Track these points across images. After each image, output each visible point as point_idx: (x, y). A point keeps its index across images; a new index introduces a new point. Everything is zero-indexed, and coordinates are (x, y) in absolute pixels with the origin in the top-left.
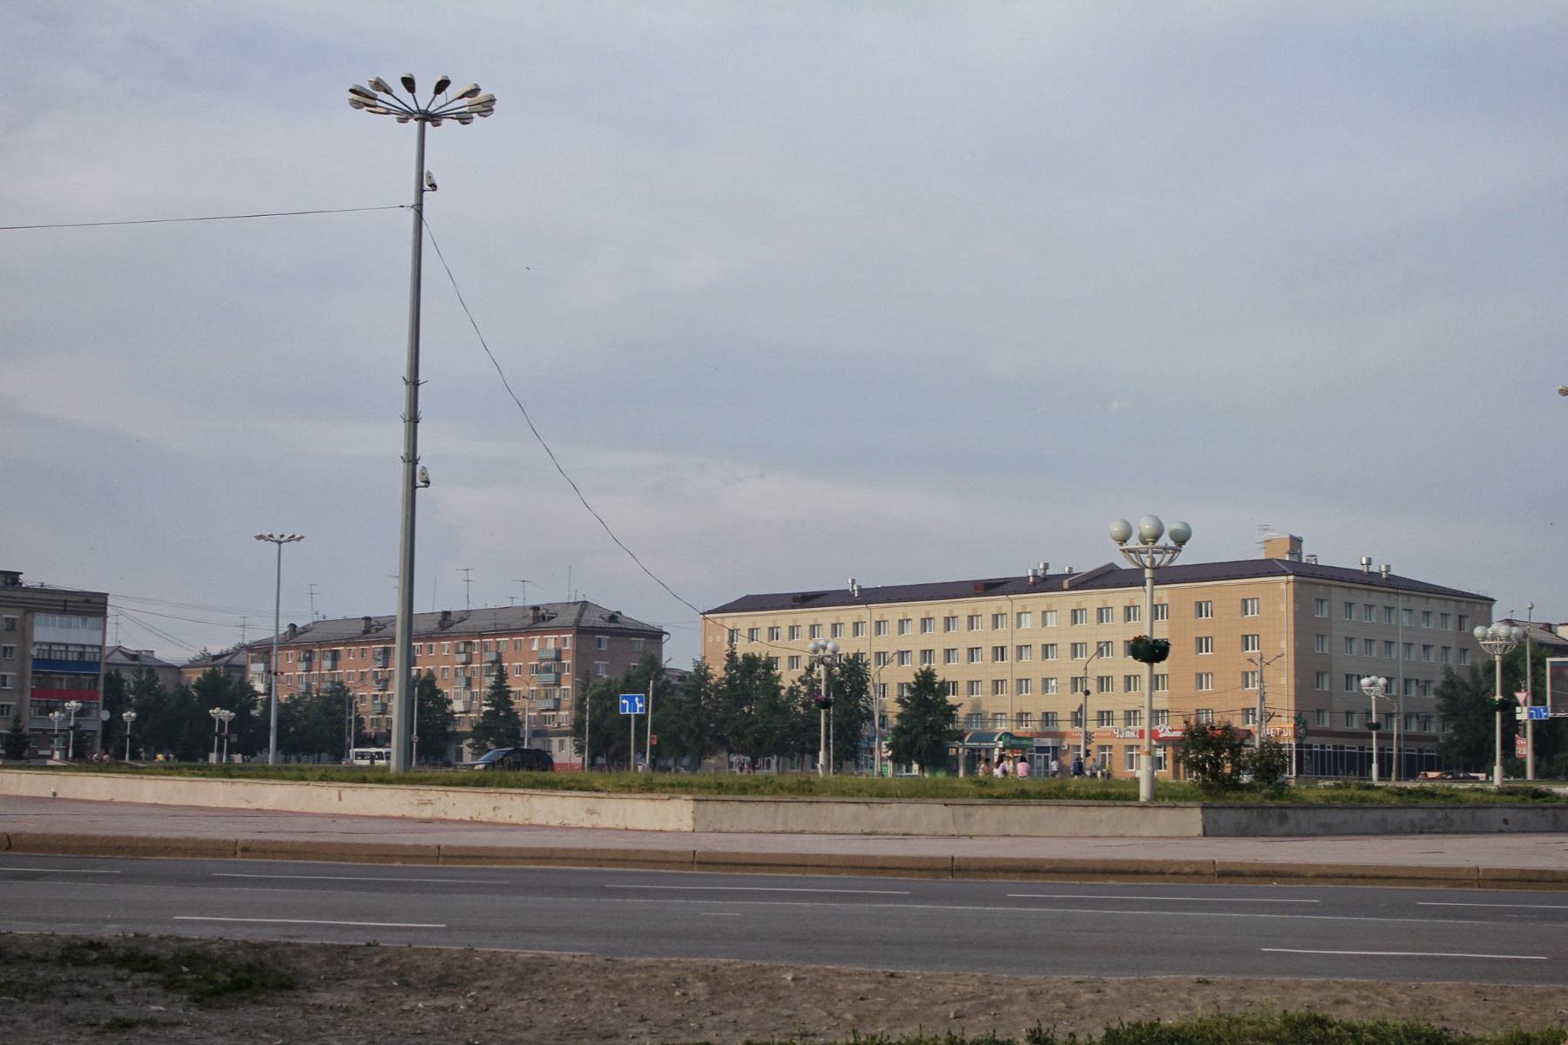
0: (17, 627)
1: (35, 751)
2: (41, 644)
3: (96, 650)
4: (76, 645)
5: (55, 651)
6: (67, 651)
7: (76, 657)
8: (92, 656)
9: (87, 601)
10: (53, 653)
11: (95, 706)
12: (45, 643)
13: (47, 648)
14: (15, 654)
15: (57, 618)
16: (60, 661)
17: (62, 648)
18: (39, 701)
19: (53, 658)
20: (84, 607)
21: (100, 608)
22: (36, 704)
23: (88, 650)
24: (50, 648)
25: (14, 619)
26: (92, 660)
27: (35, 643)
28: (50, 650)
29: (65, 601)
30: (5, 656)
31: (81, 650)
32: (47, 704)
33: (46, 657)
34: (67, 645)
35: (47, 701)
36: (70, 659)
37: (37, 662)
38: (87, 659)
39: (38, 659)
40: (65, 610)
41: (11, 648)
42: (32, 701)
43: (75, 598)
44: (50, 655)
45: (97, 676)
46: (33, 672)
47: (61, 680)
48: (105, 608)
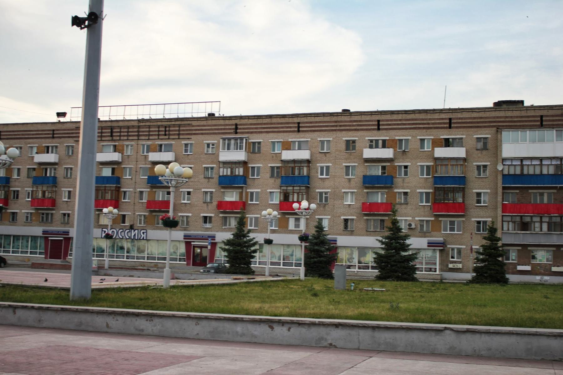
0: (489, 146)
1: (515, 265)
2: (512, 159)
5: (528, 165)
6: (541, 165)
7: (552, 171)
10: (525, 168)
13: (519, 163)
14: (488, 172)
16: (534, 175)
18: (512, 216)
19: (525, 172)
22: (509, 219)
27: (504, 160)
28: (522, 166)
30: (479, 174)
31: (554, 162)
33: (518, 172)
34: (541, 159)
36: (545, 172)
37: (506, 177)
39: (509, 175)
41: (485, 166)
42: (503, 216)
43: (551, 112)
44: (522, 170)
46: (504, 188)
47: (542, 195)
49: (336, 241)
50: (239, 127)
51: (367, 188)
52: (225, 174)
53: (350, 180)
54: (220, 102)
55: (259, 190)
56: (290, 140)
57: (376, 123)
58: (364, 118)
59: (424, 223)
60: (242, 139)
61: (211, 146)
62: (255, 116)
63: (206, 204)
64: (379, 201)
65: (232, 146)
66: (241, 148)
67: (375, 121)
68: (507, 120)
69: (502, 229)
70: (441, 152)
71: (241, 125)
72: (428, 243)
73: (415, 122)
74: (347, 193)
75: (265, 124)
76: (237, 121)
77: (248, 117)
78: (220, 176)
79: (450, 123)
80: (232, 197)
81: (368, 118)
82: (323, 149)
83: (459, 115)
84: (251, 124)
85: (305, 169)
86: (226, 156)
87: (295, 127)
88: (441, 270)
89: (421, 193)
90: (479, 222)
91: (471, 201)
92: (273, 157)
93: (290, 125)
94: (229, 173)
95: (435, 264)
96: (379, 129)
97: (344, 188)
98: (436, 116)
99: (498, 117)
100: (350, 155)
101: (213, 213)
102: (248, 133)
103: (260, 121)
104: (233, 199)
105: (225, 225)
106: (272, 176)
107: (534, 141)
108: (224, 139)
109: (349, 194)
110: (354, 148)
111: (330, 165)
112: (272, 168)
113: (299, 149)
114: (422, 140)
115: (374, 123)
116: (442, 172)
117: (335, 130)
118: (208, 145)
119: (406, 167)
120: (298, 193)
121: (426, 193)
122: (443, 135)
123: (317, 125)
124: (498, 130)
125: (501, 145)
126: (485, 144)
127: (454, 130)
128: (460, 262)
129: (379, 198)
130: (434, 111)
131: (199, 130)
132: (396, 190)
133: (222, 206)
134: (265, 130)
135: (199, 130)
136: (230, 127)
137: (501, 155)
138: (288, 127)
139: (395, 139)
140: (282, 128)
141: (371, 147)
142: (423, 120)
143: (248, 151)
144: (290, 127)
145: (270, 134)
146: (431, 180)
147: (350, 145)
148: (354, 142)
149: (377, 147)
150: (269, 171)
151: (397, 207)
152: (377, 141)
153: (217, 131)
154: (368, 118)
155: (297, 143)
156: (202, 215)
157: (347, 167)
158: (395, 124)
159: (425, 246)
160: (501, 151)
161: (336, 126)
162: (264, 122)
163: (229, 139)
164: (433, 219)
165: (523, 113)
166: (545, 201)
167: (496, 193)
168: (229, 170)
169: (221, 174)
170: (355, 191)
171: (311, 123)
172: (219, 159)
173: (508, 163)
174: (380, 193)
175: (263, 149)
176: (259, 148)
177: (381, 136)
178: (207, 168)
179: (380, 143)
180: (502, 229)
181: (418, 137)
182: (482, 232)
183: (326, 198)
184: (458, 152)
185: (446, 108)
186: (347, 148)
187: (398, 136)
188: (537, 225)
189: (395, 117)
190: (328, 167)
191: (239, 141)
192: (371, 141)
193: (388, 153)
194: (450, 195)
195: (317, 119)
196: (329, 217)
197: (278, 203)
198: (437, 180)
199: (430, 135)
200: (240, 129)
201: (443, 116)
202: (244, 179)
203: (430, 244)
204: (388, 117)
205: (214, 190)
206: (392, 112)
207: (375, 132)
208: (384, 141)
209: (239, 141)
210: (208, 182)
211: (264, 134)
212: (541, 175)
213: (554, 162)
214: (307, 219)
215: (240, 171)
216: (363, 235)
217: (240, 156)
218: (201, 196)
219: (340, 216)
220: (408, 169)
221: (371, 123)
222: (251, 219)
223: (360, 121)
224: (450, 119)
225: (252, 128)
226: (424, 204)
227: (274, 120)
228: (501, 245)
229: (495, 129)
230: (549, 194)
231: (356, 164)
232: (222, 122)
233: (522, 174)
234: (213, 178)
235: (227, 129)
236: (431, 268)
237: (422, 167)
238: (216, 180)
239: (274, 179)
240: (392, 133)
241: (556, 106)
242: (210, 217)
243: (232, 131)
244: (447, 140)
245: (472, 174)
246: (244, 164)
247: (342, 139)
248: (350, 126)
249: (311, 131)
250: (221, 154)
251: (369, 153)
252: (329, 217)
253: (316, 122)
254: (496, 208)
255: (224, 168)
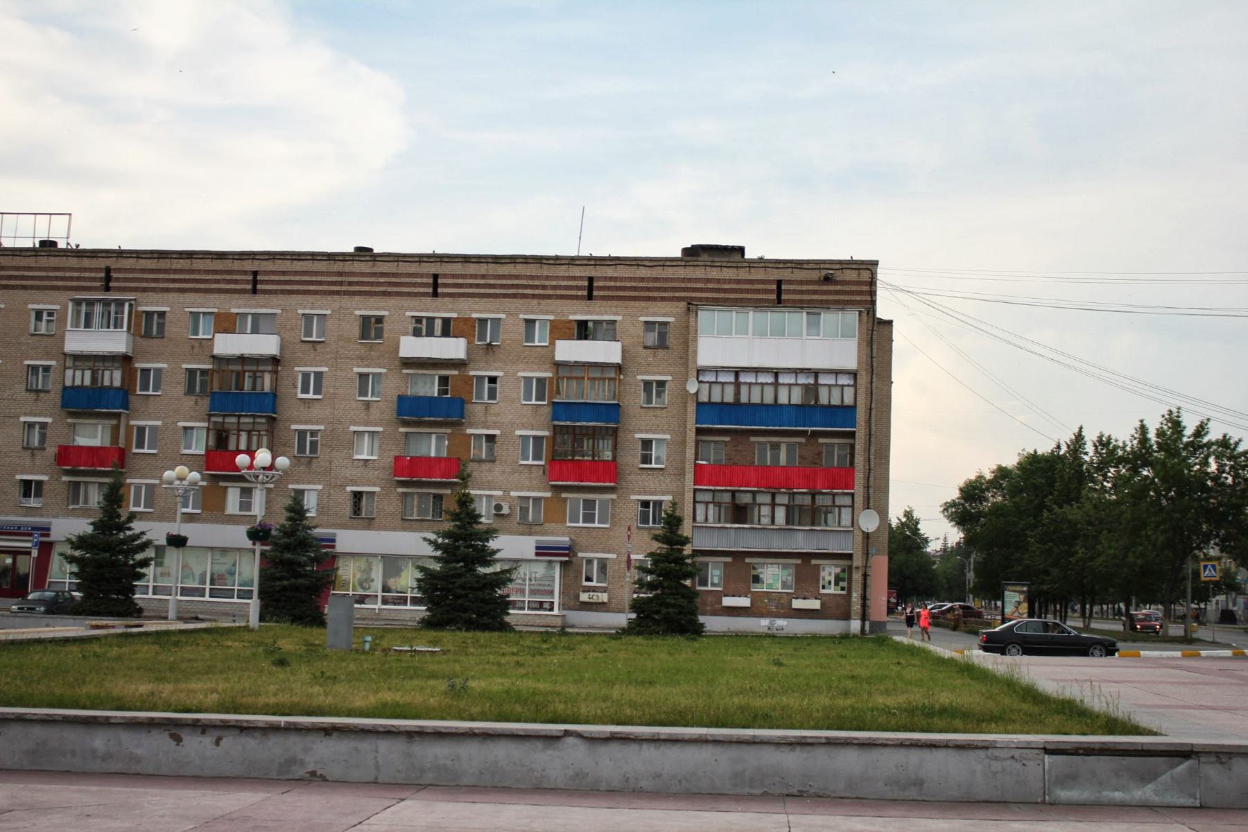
0: (671, 340)
1: (719, 596)
2: (717, 370)
3: (844, 380)
4: (796, 372)
5: (750, 384)
6: (776, 384)
7: (797, 398)
8: (836, 393)
9: (827, 280)
10: (744, 390)
11: (847, 501)
12: (725, 369)
13: (731, 379)
14: (666, 397)
15: (752, 316)
16: (762, 405)
17: (770, 379)
18: (714, 491)
19: (744, 399)
20: (815, 292)
21: (860, 293)
22: (708, 497)
23: (823, 380)
24: (737, 374)
25: (665, 324)
26: (836, 401)
27: (700, 371)
28: (737, 385)
29: (779, 283)
30: (649, 401)
31: (802, 380)
32: (733, 496)
33: (729, 398)
34: (776, 373)
35: (733, 492)
36: (783, 399)
37: (703, 407)
38: (824, 400)
39: (710, 403)
40: (779, 301)
41: (661, 384)
43: (799, 275)
44: (737, 393)
45: (852, 435)
46: (699, 432)
47: (776, 447)
48: (873, 293)
49: (334, 541)
50: (114, 275)
51: (406, 424)
52: (78, 382)
53: (368, 405)
54: (70, 214)
55: (159, 423)
56: (234, 310)
57: (431, 281)
58: (404, 268)
59: (529, 503)
60: (120, 303)
61: (45, 317)
62: (152, 252)
63: (29, 453)
64: (433, 454)
65: (96, 319)
66: (118, 324)
67: (427, 275)
68: (710, 286)
69: (694, 519)
70: (569, 350)
71: (119, 270)
72: (537, 548)
73: (515, 282)
74: (362, 433)
75: (176, 271)
76: (111, 263)
77: (138, 254)
78: (65, 388)
79: (590, 288)
80: (92, 436)
81: (412, 268)
82: (309, 334)
83: (610, 272)
84: (143, 271)
85: (267, 379)
86: (79, 341)
87: (247, 282)
88: (564, 606)
89: (525, 438)
90: (645, 504)
91: (631, 458)
92: (193, 348)
93: (235, 277)
94: (87, 382)
95: (551, 593)
96: (435, 294)
97: (355, 424)
98: (562, 271)
99: (690, 280)
100: (371, 347)
101: (46, 474)
102: (136, 290)
103: (164, 264)
104: (96, 442)
105: (76, 501)
106: (190, 390)
107: (762, 334)
108: (78, 303)
109: (366, 435)
110: (379, 334)
111: (325, 369)
112: (191, 372)
113: (255, 330)
114: (530, 323)
115: (425, 280)
116: (570, 393)
117: (338, 293)
118: (39, 315)
119: (493, 380)
120: (249, 432)
121: (535, 437)
122: (575, 313)
123: (297, 278)
124: (692, 306)
125: (696, 340)
126: (662, 336)
127: (599, 303)
128: (604, 590)
129: (432, 446)
130: (557, 260)
131: (16, 278)
132: (469, 431)
133: (67, 456)
134: (177, 285)
135: (16, 278)
136: (93, 275)
137: (695, 361)
138: (229, 282)
139: (471, 319)
140: (217, 281)
141: (417, 333)
142: (532, 278)
143: (133, 331)
144: (236, 282)
145: (186, 295)
146: (547, 411)
147: (371, 327)
148: (380, 320)
149: (430, 333)
150: (183, 378)
151: (471, 467)
152: (431, 320)
153: (60, 283)
154: (412, 268)
155: (250, 318)
156: (18, 477)
157: (363, 377)
158: (471, 286)
159: (530, 553)
160: (695, 352)
161: (341, 283)
162: (174, 267)
163: (91, 303)
164: (549, 495)
165: (743, 274)
166: (783, 460)
167: (684, 442)
168: (88, 374)
169: (68, 383)
170: (380, 429)
171: (284, 273)
172: (63, 348)
173: (710, 377)
174: (434, 437)
175: (170, 329)
176: (161, 327)
177: (441, 311)
178: (35, 369)
179: (438, 325)
180: (694, 519)
181: (522, 316)
182: (651, 525)
183: (314, 445)
184: (605, 351)
185: (582, 254)
186: (365, 334)
187: (477, 311)
188: (765, 511)
189: (472, 269)
190: (319, 375)
191: (113, 308)
192: (418, 320)
193: (454, 348)
194: (587, 444)
195: (299, 266)
196: (320, 487)
197: (203, 452)
198: (559, 410)
199: (547, 313)
200: (118, 280)
201: (577, 271)
202: (124, 396)
203: (542, 550)
204: (457, 268)
205: (49, 420)
206: (466, 259)
207: (429, 299)
208: (446, 322)
209: (113, 308)
210: (36, 400)
211: (175, 295)
212: (776, 404)
213: (802, 380)
214: (269, 490)
215: (113, 378)
216: (394, 529)
217: (115, 342)
218: (18, 432)
219: (343, 486)
220: (498, 385)
221: (419, 280)
222: (138, 488)
223: (395, 275)
224: (591, 280)
225: (147, 280)
226: (530, 462)
227: (199, 264)
228: (690, 553)
229: (683, 304)
230: (788, 444)
231: (383, 371)
232: (73, 262)
233: (737, 403)
234: (48, 392)
235: (84, 279)
236: (541, 603)
237: (528, 380)
238: (55, 395)
239: (194, 398)
240: (464, 303)
241: (808, 262)
242: (39, 484)
243: (98, 284)
244: (582, 325)
245: (634, 399)
246: (125, 360)
247: (352, 314)
248: (372, 284)
249: (283, 292)
250: (68, 336)
251: (412, 347)
252: (320, 487)
253: (296, 273)
254: (682, 473)
255: (75, 368)
